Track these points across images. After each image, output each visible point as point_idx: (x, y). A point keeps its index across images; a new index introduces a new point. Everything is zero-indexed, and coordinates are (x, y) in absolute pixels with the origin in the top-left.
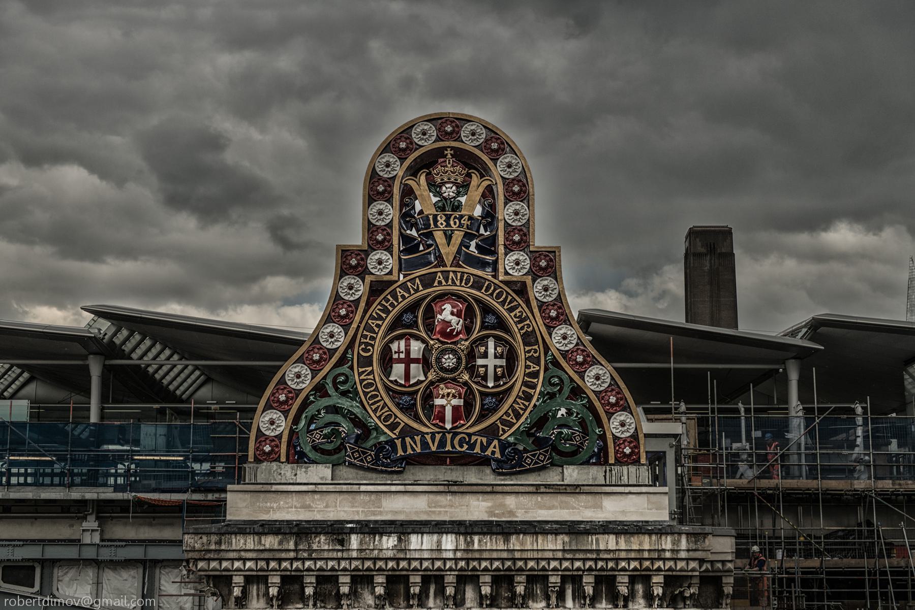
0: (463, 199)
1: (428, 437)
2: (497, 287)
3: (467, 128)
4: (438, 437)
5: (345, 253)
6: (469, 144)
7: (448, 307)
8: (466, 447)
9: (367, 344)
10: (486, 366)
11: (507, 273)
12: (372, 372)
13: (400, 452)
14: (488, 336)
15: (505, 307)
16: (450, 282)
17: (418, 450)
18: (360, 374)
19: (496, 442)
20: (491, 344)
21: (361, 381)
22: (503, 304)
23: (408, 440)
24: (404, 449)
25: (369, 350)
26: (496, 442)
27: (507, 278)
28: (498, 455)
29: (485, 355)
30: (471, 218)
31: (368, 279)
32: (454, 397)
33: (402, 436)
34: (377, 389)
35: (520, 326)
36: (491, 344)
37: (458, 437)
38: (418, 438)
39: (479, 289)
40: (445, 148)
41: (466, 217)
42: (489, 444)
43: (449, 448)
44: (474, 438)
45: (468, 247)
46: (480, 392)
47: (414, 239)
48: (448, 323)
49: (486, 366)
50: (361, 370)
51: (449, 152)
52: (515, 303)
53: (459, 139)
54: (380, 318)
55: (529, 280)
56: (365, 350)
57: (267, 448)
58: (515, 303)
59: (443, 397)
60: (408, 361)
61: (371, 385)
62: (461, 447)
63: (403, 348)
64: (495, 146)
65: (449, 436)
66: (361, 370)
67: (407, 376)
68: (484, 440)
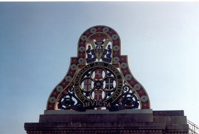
0: (103, 45)
1: (92, 102)
2: (111, 66)
3: (104, 29)
4: (94, 102)
5: (73, 59)
6: (104, 32)
7: (98, 71)
8: (101, 104)
9: (77, 81)
10: (108, 85)
11: (113, 62)
12: (78, 87)
13: (84, 106)
14: (108, 78)
15: (113, 70)
16: (98, 65)
17: (89, 106)
18: (75, 87)
19: (109, 103)
20: (109, 79)
21: (75, 89)
22: (112, 70)
23: (86, 103)
24: (85, 105)
25: (77, 82)
26: (109, 103)
27: (114, 63)
28: (110, 106)
29: (108, 82)
30: (105, 49)
31: (78, 65)
32: (99, 93)
33: (85, 102)
34: (79, 91)
35: (116, 74)
36: (109, 79)
37: (100, 102)
38: (89, 103)
39: (107, 67)
40: (98, 33)
41: (104, 49)
42: (108, 103)
43: (97, 105)
44: (103, 102)
45: (104, 56)
46: (106, 91)
47: (91, 55)
48: (98, 75)
49: (108, 85)
50: (75, 86)
51: (99, 34)
52: (115, 69)
53: (102, 31)
54: (80, 75)
55: (119, 63)
56: (77, 82)
57: (51, 106)
58: (115, 69)
59: (97, 93)
60: (87, 85)
61: (78, 90)
62: (100, 104)
63: (86, 81)
64: (111, 32)
65: (97, 102)
66: (75, 86)
67: (88, 89)
68: (106, 103)
